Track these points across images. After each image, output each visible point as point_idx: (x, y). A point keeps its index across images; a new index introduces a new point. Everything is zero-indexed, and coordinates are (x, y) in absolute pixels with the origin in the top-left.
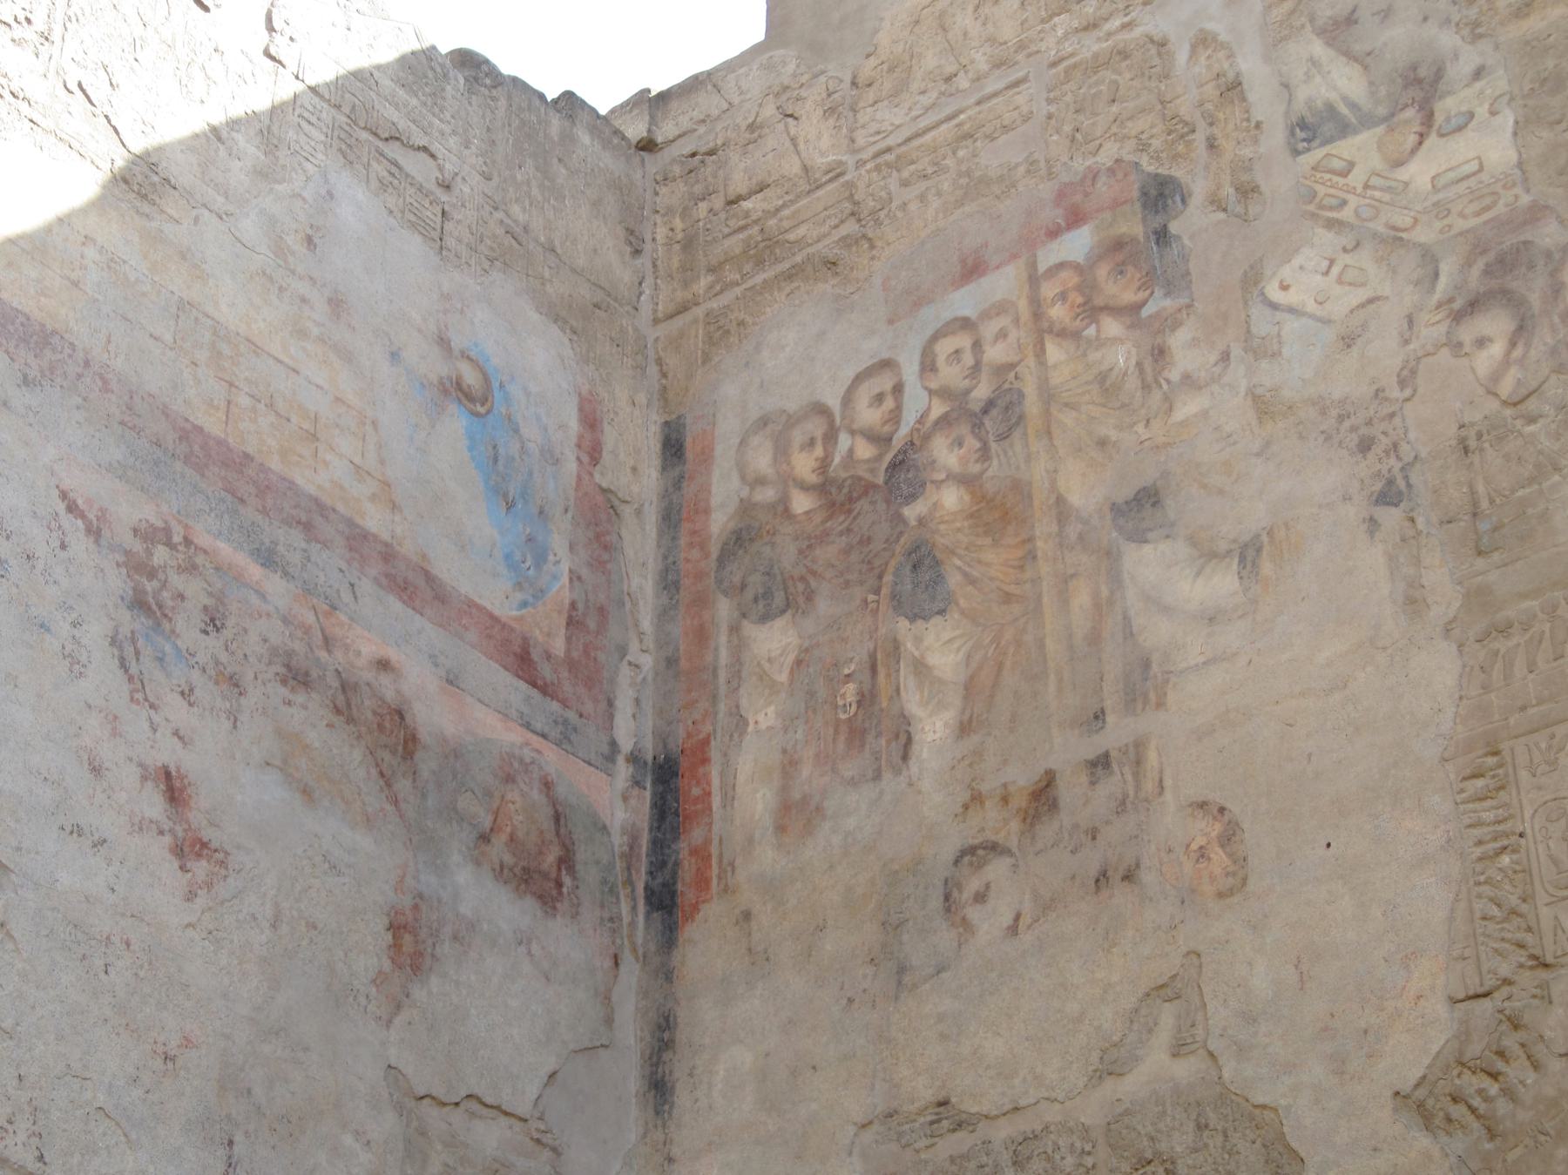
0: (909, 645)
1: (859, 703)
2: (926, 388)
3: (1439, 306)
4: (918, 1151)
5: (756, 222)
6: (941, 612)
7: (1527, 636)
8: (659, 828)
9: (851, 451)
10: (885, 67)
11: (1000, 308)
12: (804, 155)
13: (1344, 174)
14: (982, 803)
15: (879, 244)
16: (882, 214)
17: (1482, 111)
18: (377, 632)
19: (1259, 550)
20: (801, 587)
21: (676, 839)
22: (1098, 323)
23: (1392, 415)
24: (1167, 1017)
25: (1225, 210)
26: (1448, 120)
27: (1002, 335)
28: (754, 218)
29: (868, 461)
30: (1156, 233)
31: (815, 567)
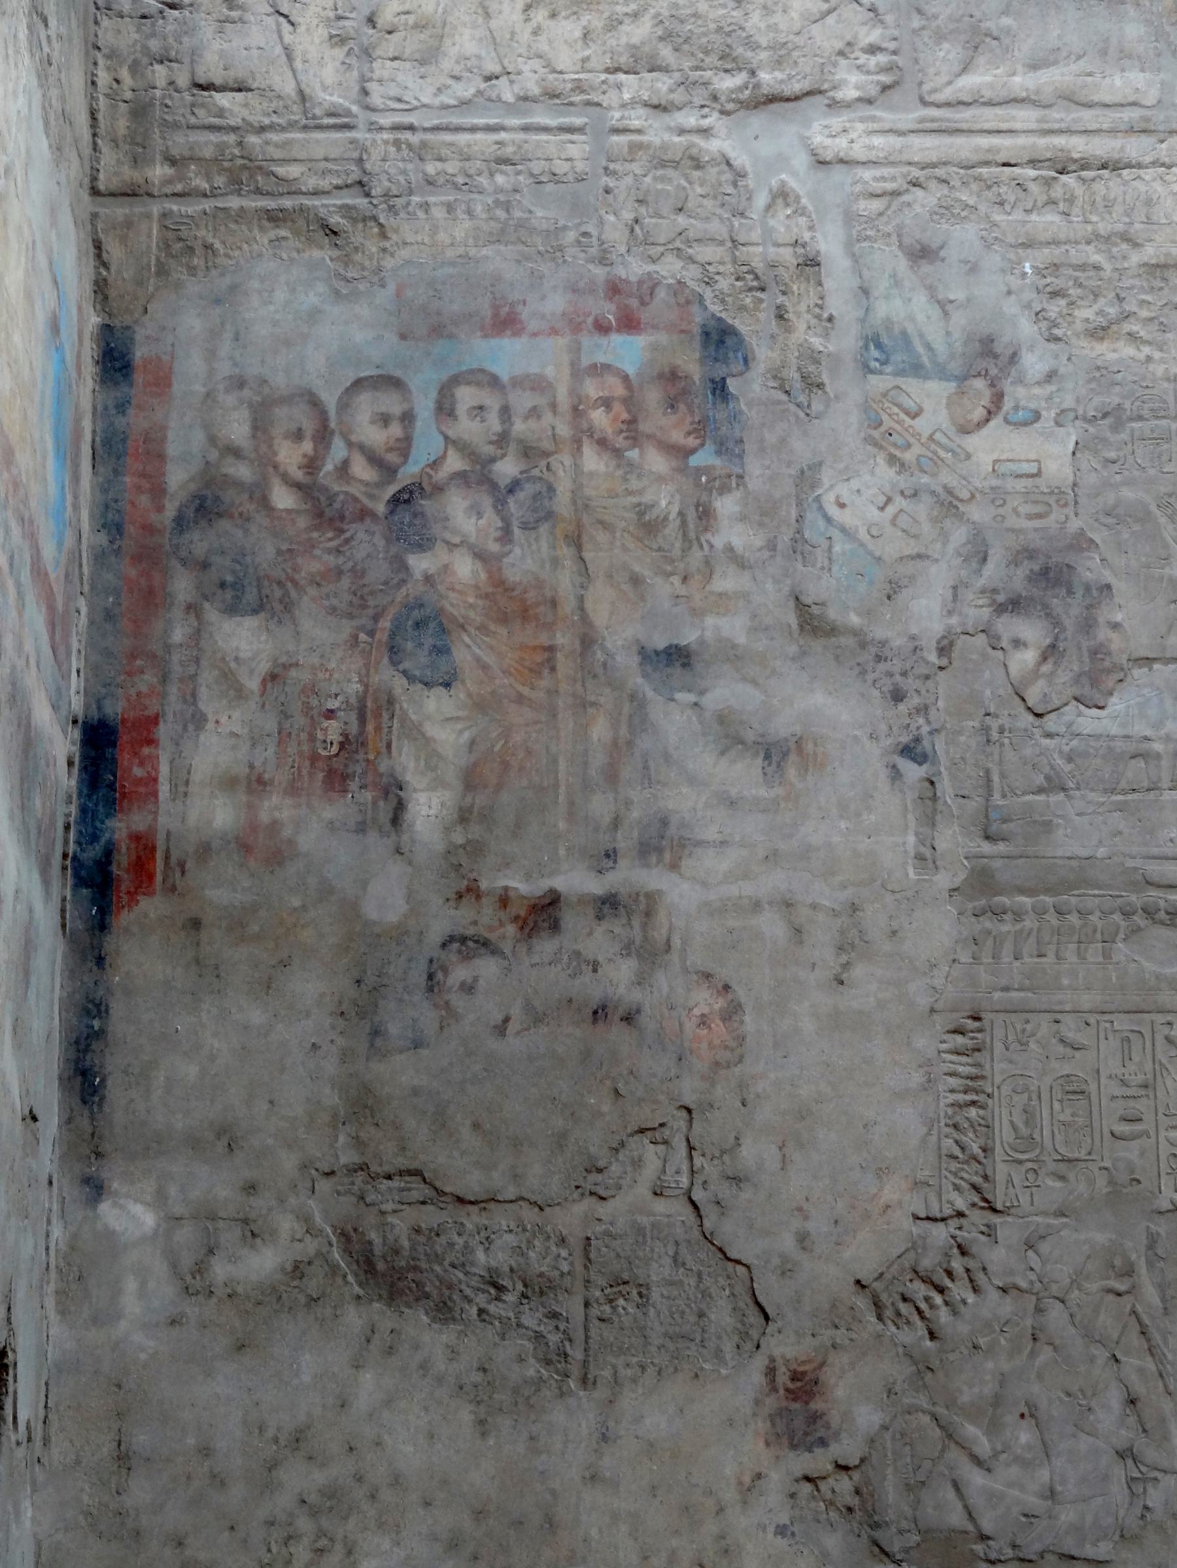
0: (405, 705)
1: (342, 746)
2: (442, 433)
3: (983, 592)
4: (383, 1213)
5: (234, 129)
6: (447, 685)
7: (1018, 927)
10: (411, 19)
11: (538, 384)
12: (301, 77)
13: (914, 416)
14: (478, 897)
15: (394, 237)
16: (399, 202)
17: (1049, 415)
19: (785, 754)
20: (278, 593)
23: (927, 677)
24: (651, 1154)
26: (1016, 408)
28: (232, 123)
29: (367, 484)
30: (712, 381)
31: (297, 577)
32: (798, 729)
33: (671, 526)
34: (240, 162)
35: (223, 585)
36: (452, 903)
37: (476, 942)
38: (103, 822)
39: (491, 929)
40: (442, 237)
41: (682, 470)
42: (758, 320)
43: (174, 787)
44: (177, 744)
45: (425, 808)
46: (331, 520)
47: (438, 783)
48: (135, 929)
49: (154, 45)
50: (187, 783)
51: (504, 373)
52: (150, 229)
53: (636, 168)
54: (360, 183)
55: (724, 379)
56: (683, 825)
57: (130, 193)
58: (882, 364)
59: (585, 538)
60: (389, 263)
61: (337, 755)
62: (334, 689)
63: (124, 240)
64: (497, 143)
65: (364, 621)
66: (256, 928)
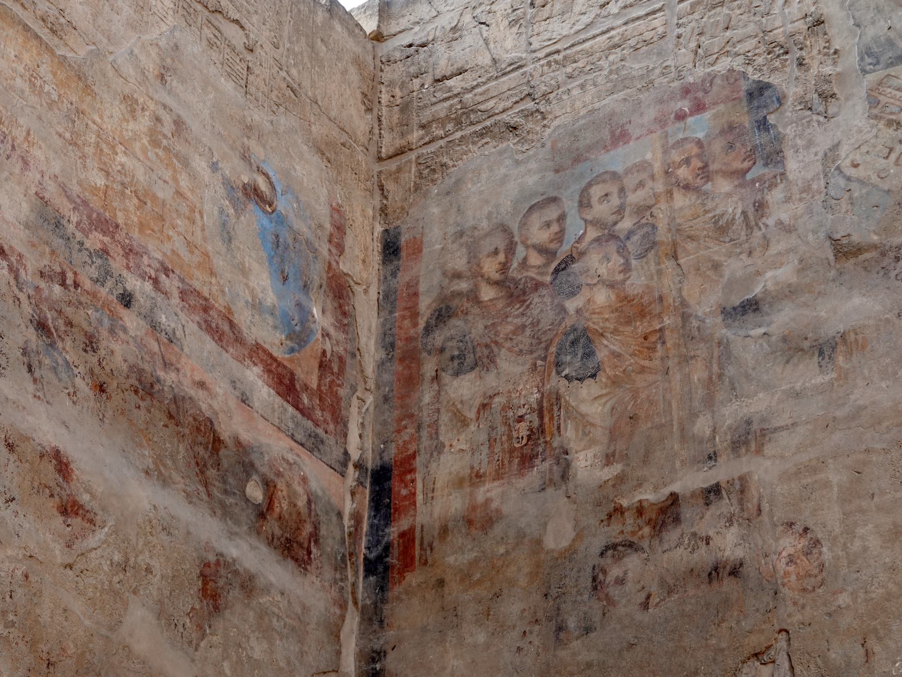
0: (567, 398)
1: (529, 438)
2: (583, 219)
6: (593, 376)
8: (375, 516)
9: (525, 259)
11: (643, 166)
14: (622, 513)
16: (552, 96)
19: (834, 349)
20: (486, 352)
21: (387, 525)
22: (712, 180)
25: (810, 109)
27: (641, 184)
28: (455, 92)
30: (757, 121)
31: (497, 339)
32: (841, 328)
33: (737, 223)
34: (460, 112)
35: (452, 359)
36: (605, 523)
37: (623, 546)
38: (383, 531)
39: (633, 533)
40: (578, 104)
41: (741, 186)
42: (785, 72)
43: (425, 494)
44: (427, 467)
45: (583, 462)
46: (519, 296)
47: (592, 442)
48: (404, 597)
49: (413, 70)
50: (433, 491)
51: (619, 169)
52: (411, 168)
53: (696, 16)
54: (529, 95)
55: (765, 117)
56: (763, 420)
57: (400, 152)
58: (874, 66)
59: (679, 251)
60: (548, 131)
61: (525, 445)
62: (522, 402)
63: (396, 180)
64: (609, 38)
65: (541, 353)
66: (478, 576)
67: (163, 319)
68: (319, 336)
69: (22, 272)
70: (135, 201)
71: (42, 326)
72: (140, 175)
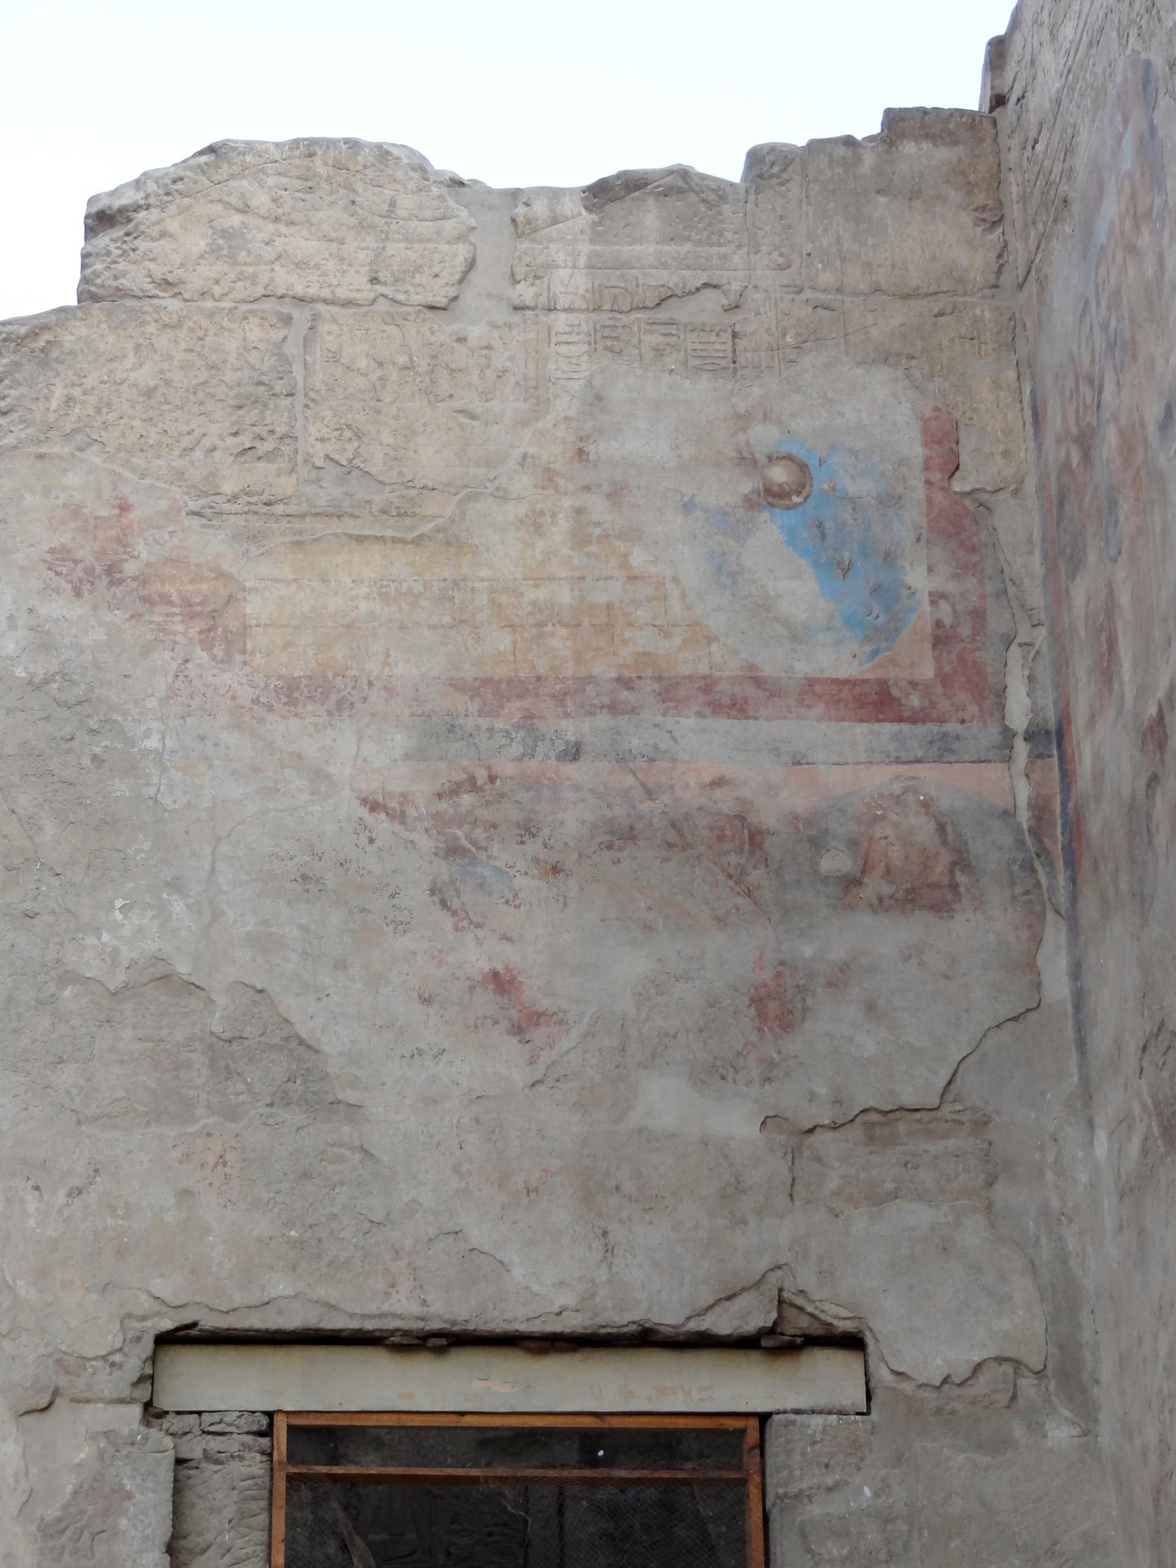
18: (705, 757)
67: (635, 742)
68: (926, 607)
69: (411, 812)
70: (562, 631)
71: (453, 851)
72: (565, 596)
